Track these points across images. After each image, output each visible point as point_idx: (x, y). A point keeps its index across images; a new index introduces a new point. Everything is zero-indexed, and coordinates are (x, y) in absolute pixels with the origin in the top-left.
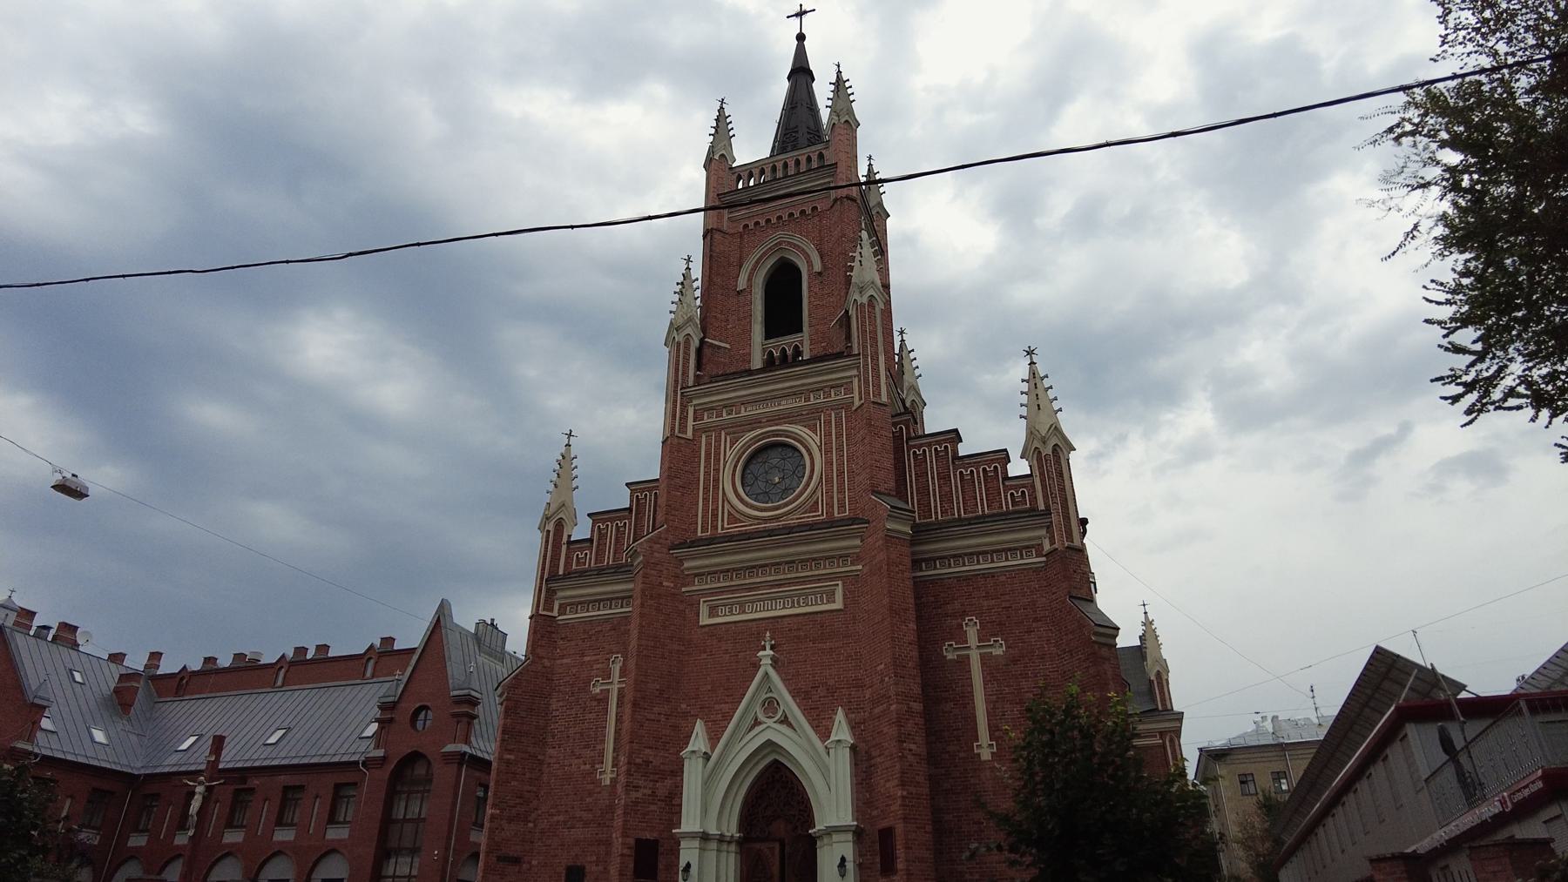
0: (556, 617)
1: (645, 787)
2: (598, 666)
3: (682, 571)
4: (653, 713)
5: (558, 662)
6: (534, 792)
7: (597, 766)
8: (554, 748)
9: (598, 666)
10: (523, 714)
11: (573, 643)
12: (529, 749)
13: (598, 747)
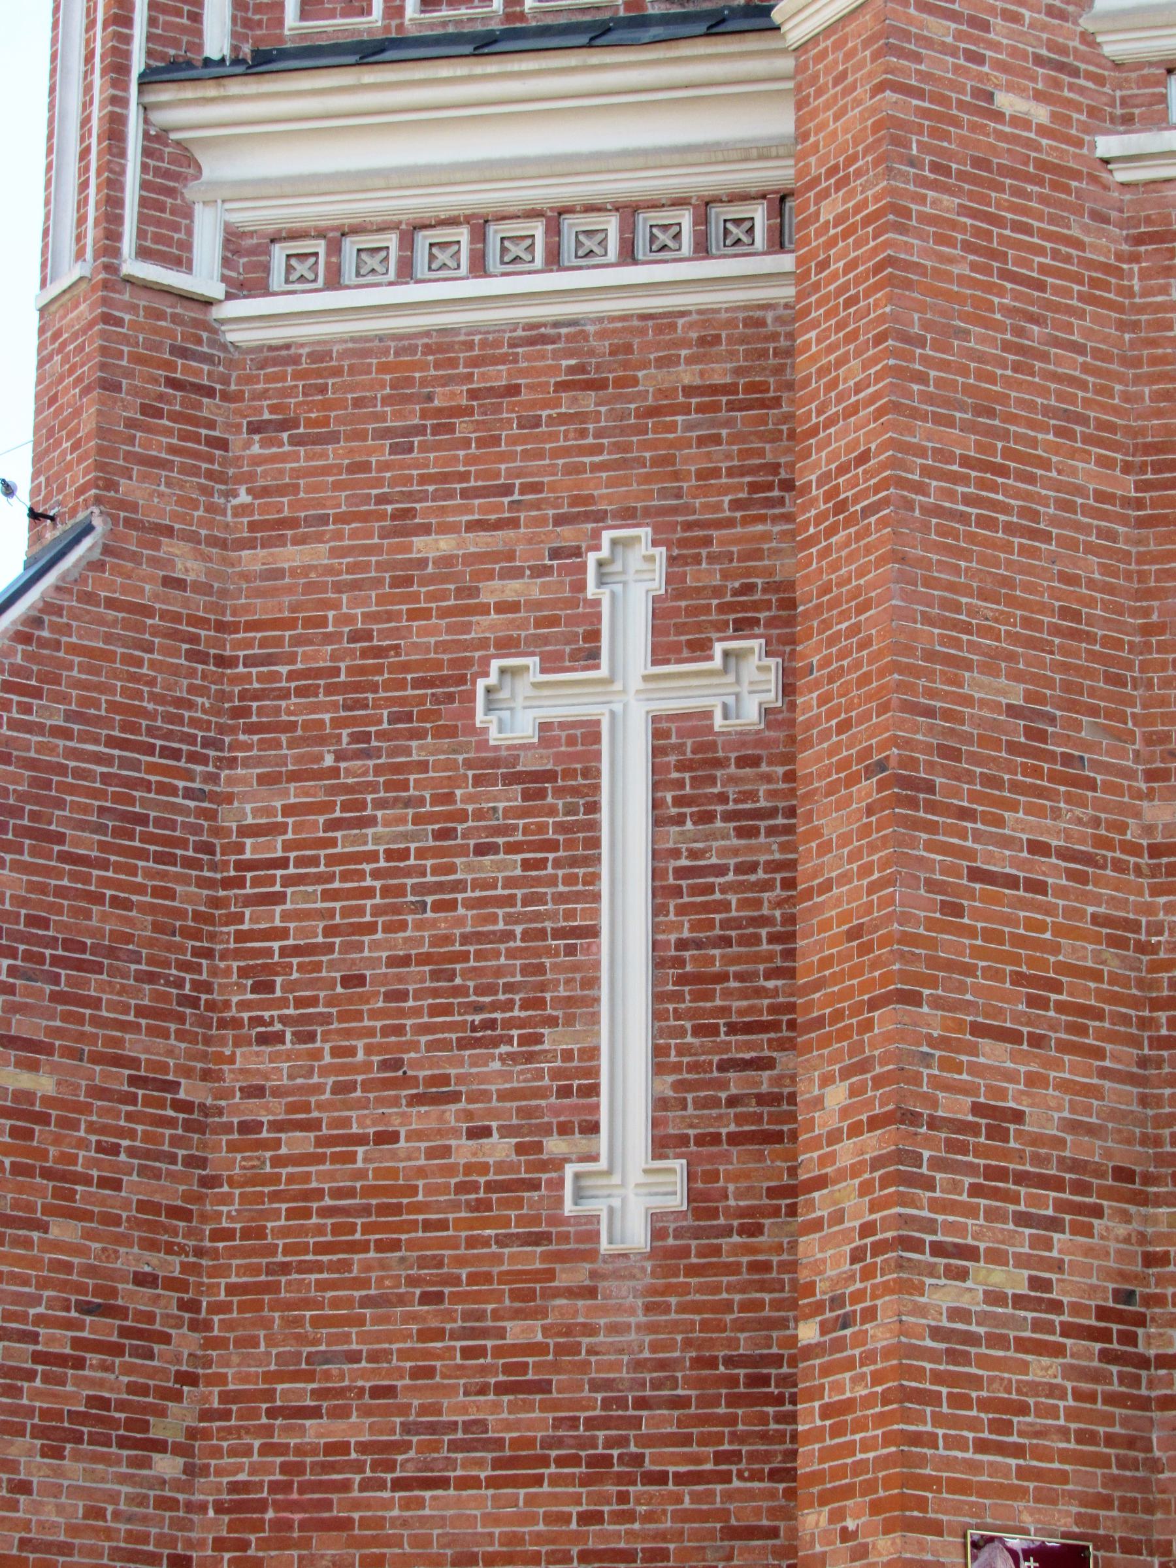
0: (208, 303)
1: (997, 1257)
2: (512, 589)
3: (1087, 38)
4: (1007, 842)
5: (252, 560)
6: (173, 1284)
7: (555, 1145)
8: (279, 1038)
9: (512, 589)
10: (87, 844)
11: (333, 454)
12: (136, 1045)
13: (553, 1040)
